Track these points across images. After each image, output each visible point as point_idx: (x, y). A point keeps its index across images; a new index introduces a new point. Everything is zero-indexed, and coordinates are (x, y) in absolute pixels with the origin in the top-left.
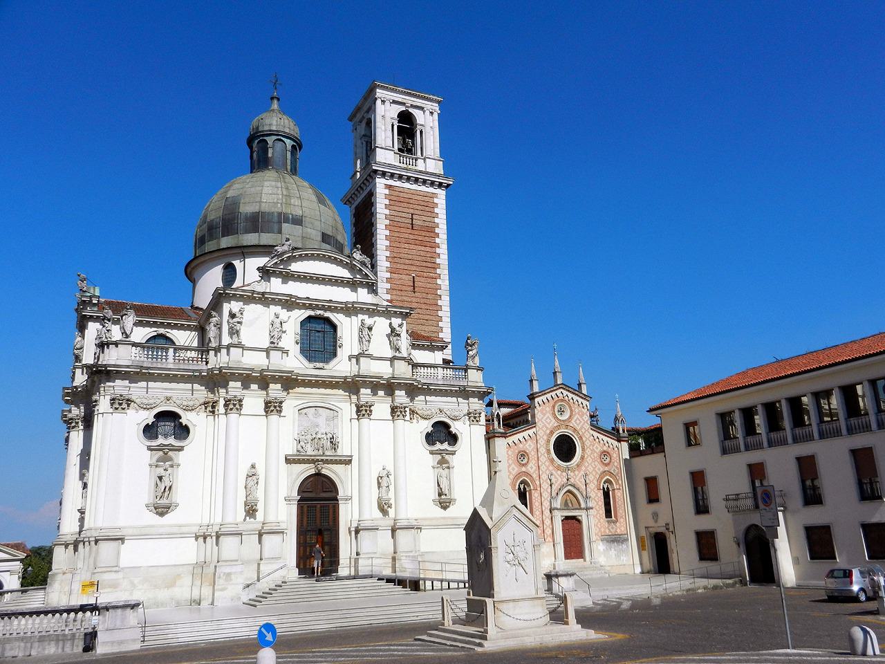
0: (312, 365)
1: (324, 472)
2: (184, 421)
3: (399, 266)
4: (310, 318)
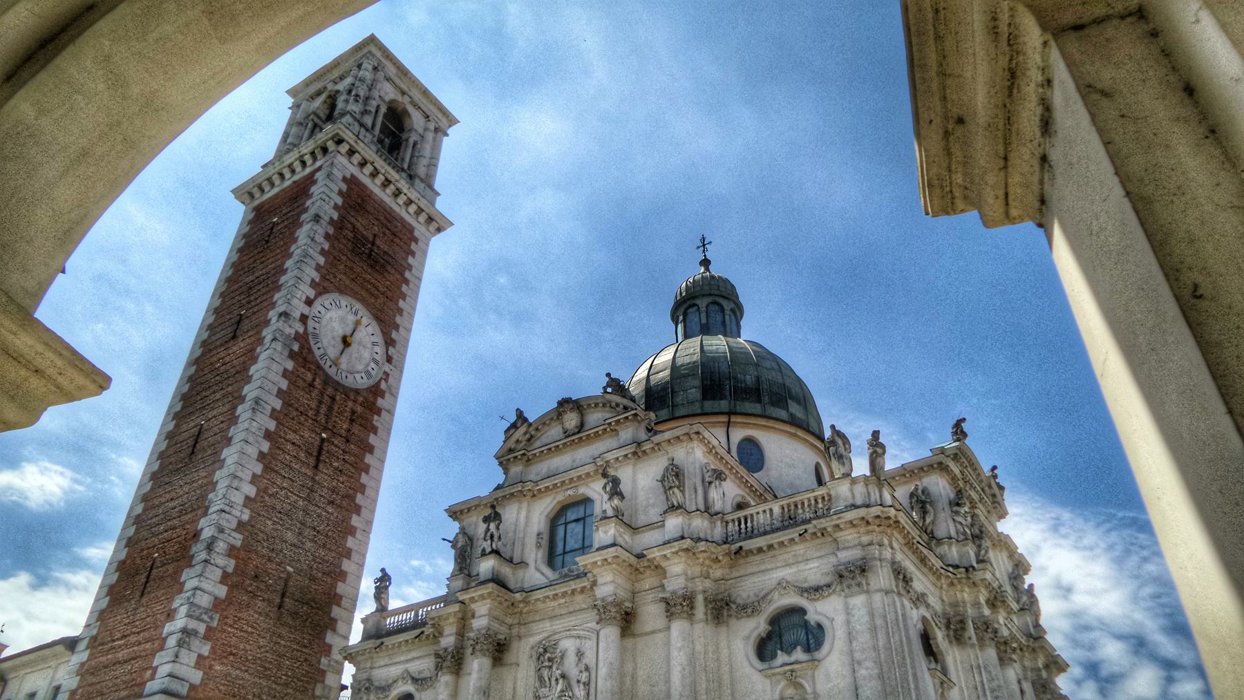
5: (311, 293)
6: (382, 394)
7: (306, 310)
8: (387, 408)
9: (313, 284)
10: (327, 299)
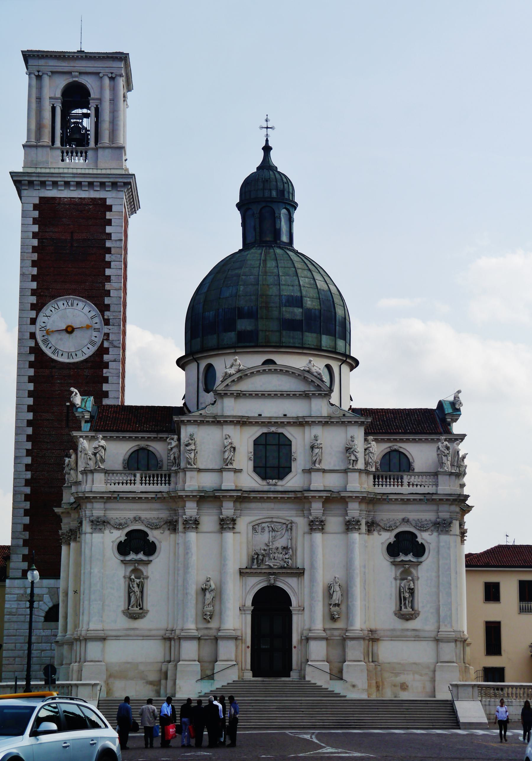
0: (264, 483)
1: (279, 584)
2: (151, 538)
4: (265, 435)
5: (33, 314)
6: (106, 351)
7: (32, 328)
8: (113, 359)
9: (33, 307)
10: (47, 310)
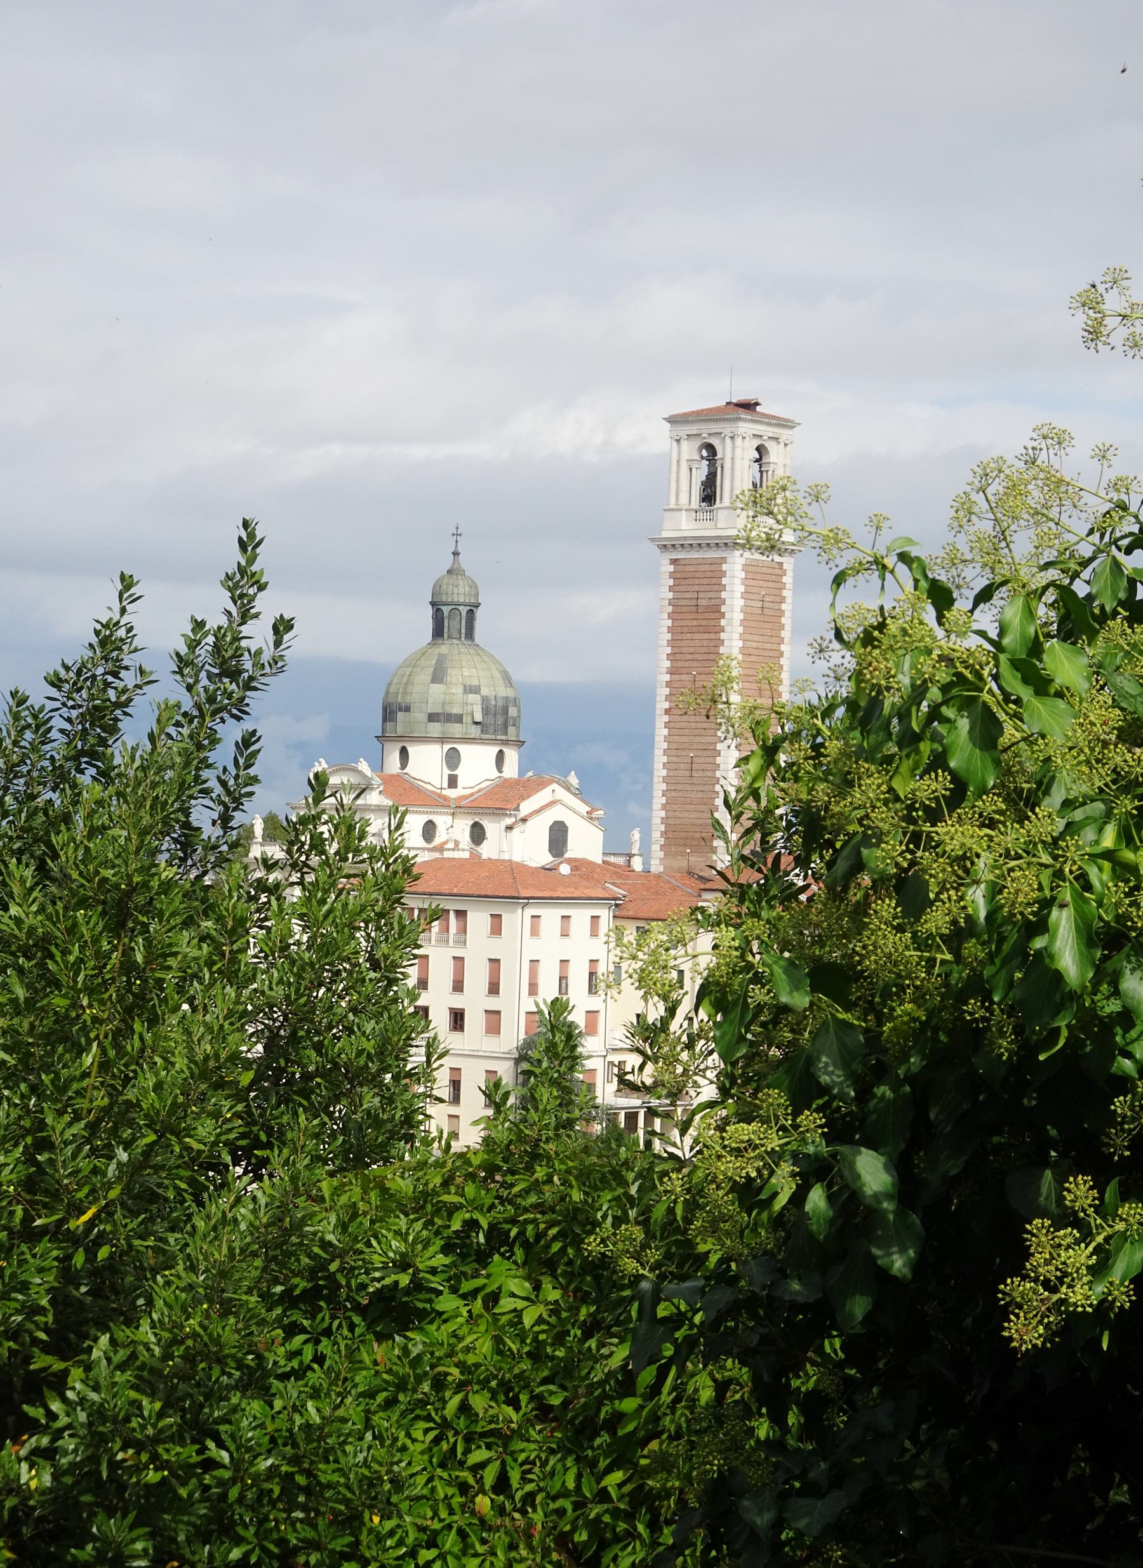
3: (680, 664)
